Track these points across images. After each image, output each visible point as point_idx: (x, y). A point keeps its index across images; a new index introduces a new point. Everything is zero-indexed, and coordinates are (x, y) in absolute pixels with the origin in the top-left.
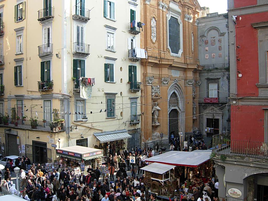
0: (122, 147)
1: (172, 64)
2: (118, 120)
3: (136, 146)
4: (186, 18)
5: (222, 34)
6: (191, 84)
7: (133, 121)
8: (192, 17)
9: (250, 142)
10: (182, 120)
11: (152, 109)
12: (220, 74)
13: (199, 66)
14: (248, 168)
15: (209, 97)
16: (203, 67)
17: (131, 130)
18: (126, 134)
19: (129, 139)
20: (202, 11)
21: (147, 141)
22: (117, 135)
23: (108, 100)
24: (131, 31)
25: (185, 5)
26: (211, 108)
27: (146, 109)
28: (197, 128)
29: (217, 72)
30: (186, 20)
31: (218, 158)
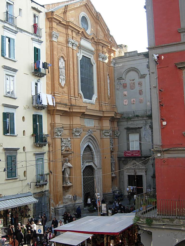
0: (26, 215)
1: (85, 112)
2: (21, 181)
3: (44, 212)
4: (100, 58)
5: (143, 76)
6: (109, 135)
7: (39, 184)
8: (108, 57)
9: (179, 201)
10: (99, 178)
11: (62, 166)
12: (142, 122)
13: (117, 113)
14: (178, 233)
15: (130, 150)
16: (122, 114)
17: (37, 193)
18: (31, 199)
19: (35, 204)
20: (118, 49)
21: (57, 205)
22: (20, 201)
23: (8, 157)
24: (36, 73)
25: (99, 42)
26: (132, 163)
27: (55, 166)
28: (117, 188)
29: (138, 120)
30: (101, 59)
31: (143, 222)
